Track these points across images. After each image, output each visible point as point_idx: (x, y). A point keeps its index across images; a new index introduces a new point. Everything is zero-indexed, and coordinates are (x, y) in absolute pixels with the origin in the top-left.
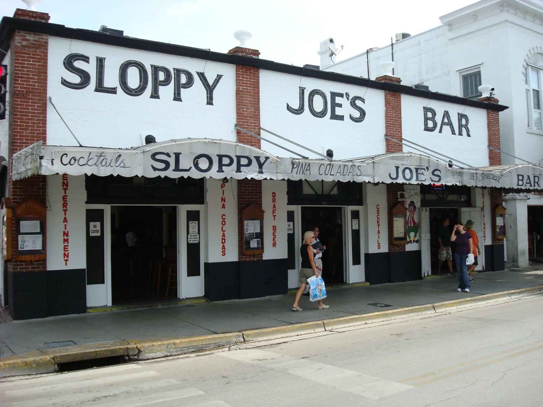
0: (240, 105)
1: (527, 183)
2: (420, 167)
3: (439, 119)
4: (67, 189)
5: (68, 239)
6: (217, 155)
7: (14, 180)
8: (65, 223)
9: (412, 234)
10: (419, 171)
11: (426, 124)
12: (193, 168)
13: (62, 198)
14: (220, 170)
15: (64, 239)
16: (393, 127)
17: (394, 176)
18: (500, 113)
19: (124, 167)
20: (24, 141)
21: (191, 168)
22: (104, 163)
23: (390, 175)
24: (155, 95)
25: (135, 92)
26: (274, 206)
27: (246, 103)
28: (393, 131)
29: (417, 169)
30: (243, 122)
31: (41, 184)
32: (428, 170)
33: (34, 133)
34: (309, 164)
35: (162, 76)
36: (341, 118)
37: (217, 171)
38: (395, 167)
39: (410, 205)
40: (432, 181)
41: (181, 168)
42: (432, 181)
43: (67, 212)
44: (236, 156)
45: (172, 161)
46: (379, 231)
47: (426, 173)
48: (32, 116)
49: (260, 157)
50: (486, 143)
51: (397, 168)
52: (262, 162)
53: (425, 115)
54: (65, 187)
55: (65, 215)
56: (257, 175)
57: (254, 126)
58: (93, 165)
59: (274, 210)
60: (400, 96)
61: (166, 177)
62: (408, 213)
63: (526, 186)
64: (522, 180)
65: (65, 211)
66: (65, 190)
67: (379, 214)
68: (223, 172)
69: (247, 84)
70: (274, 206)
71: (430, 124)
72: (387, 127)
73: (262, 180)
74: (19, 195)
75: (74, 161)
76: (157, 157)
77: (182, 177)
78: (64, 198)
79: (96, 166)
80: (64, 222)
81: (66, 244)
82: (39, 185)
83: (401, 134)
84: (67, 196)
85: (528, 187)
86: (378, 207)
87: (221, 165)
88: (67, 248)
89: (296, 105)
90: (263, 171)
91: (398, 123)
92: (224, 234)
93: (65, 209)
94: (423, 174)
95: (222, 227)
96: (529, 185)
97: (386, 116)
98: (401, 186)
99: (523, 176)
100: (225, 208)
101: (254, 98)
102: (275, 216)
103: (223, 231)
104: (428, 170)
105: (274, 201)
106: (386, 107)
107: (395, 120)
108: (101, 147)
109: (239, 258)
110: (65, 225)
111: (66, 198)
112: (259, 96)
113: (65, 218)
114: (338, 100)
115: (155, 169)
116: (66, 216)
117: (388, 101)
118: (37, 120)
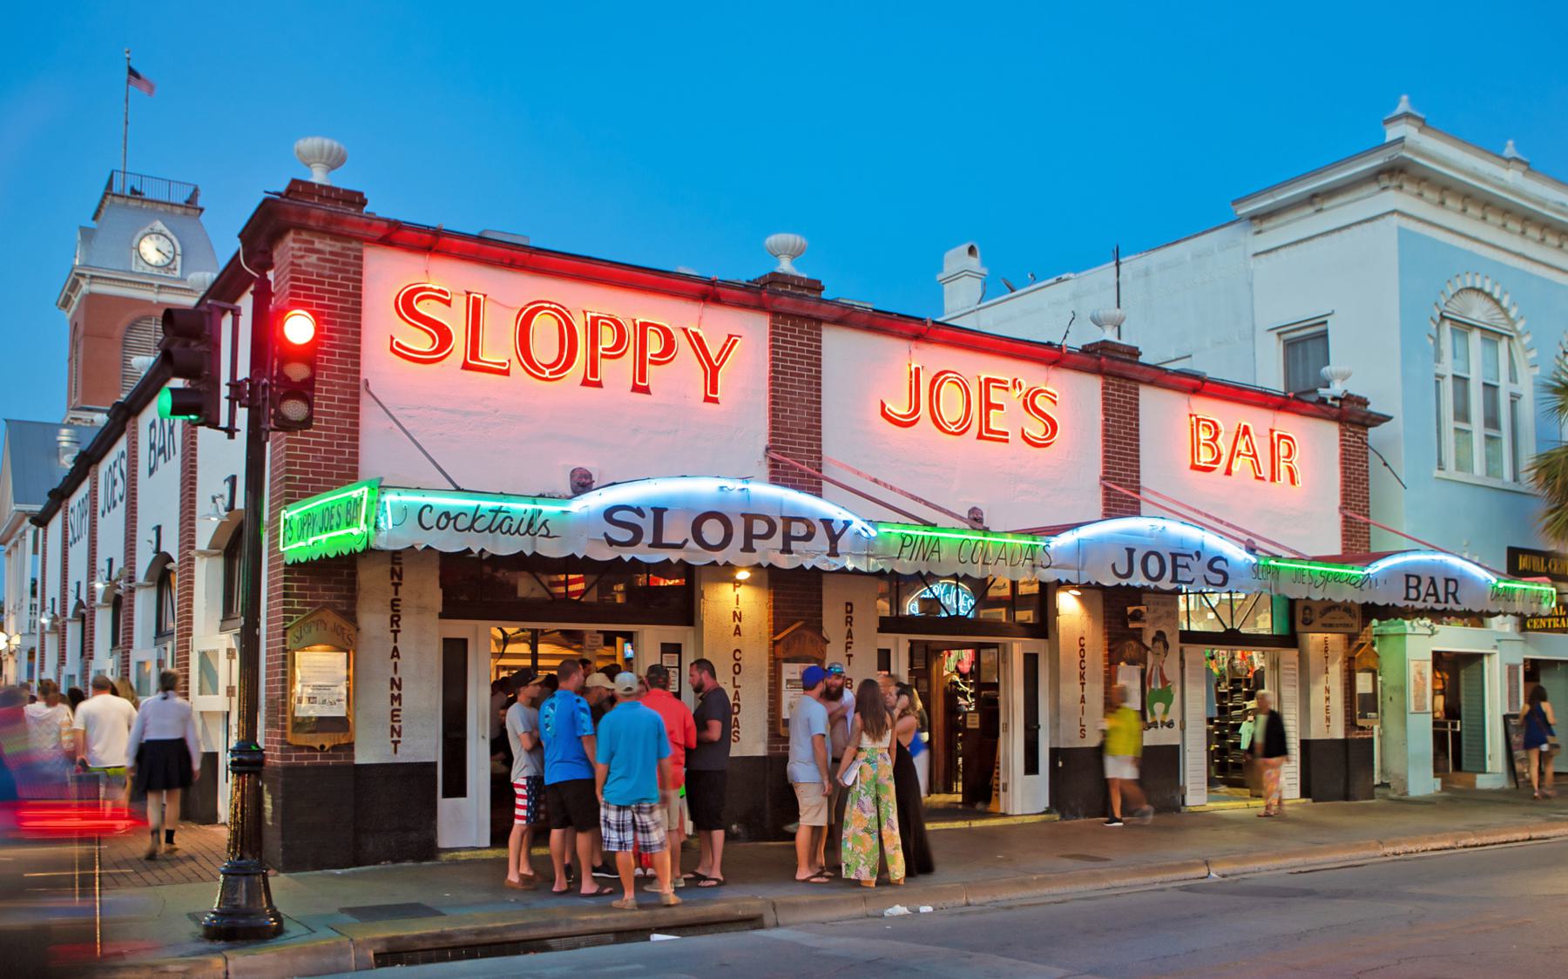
0: (777, 404)
1: (1427, 594)
2: (1181, 551)
3: (1224, 444)
4: (401, 584)
5: (400, 695)
6: (743, 515)
7: (289, 563)
8: (395, 659)
10: (1180, 561)
11: (1194, 453)
12: (692, 544)
13: (389, 603)
15: (393, 695)
16: (1119, 459)
17: (1123, 570)
18: (1371, 430)
19: (547, 536)
20: (311, 476)
21: (686, 541)
22: (505, 528)
23: (1113, 566)
24: (591, 381)
25: (551, 373)
26: (850, 635)
27: (791, 399)
28: (1120, 469)
29: (1174, 556)
30: (783, 442)
31: (345, 571)
32: (1199, 559)
33: (332, 460)
34: (938, 539)
35: (607, 338)
36: (1002, 437)
37: (742, 550)
38: (1127, 549)
39: (1154, 640)
40: (1208, 582)
41: (665, 540)
42: (1208, 582)
43: (399, 635)
44: (782, 517)
45: (647, 525)
46: (1083, 697)
47: (1193, 563)
48: (326, 421)
49: (832, 520)
50: (1337, 500)
51: (1131, 551)
52: (837, 533)
53: (1194, 432)
54: (396, 580)
55: (396, 641)
56: (826, 561)
57: (808, 451)
58: (485, 530)
59: (848, 643)
60: (1138, 389)
61: (633, 559)
62: (1150, 658)
63: (1424, 601)
64: (1417, 588)
65: (395, 632)
66: (397, 585)
67: (1085, 659)
68: (754, 551)
69: (794, 356)
70: (850, 635)
71: (1205, 457)
72: (1107, 458)
73: (825, 577)
74: (296, 596)
75: (446, 521)
76: (617, 516)
77: (668, 561)
78: (394, 604)
79: (491, 532)
80: (393, 656)
81: (396, 705)
82: (342, 575)
83: (1138, 477)
84: (399, 600)
85: (1431, 601)
86: (1082, 642)
87: (749, 536)
88: (398, 716)
89: (900, 408)
90: (839, 551)
91: (1131, 450)
92: (737, 693)
93: (395, 628)
94: (1187, 566)
95: (734, 678)
96: (1434, 598)
97: (1107, 434)
98: (1136, 594)
99: (1418, 578)
100: (740, 634)
101: (811, 389)
102: (851, 655)
103: (735, 686)
104: (1199, 559)
105: (849, 621)
106: (1105, 414)
107: (1125, 444)
108: (501, 493)
109: (770, 748)
110: (396, 664)
111: (398, 605)
112: (819, 384)
113: (395, 649)
114: (996, 396)
115: (611, 542)
116: (397, 644)
117: (1108, 399)
118: (339, 430)
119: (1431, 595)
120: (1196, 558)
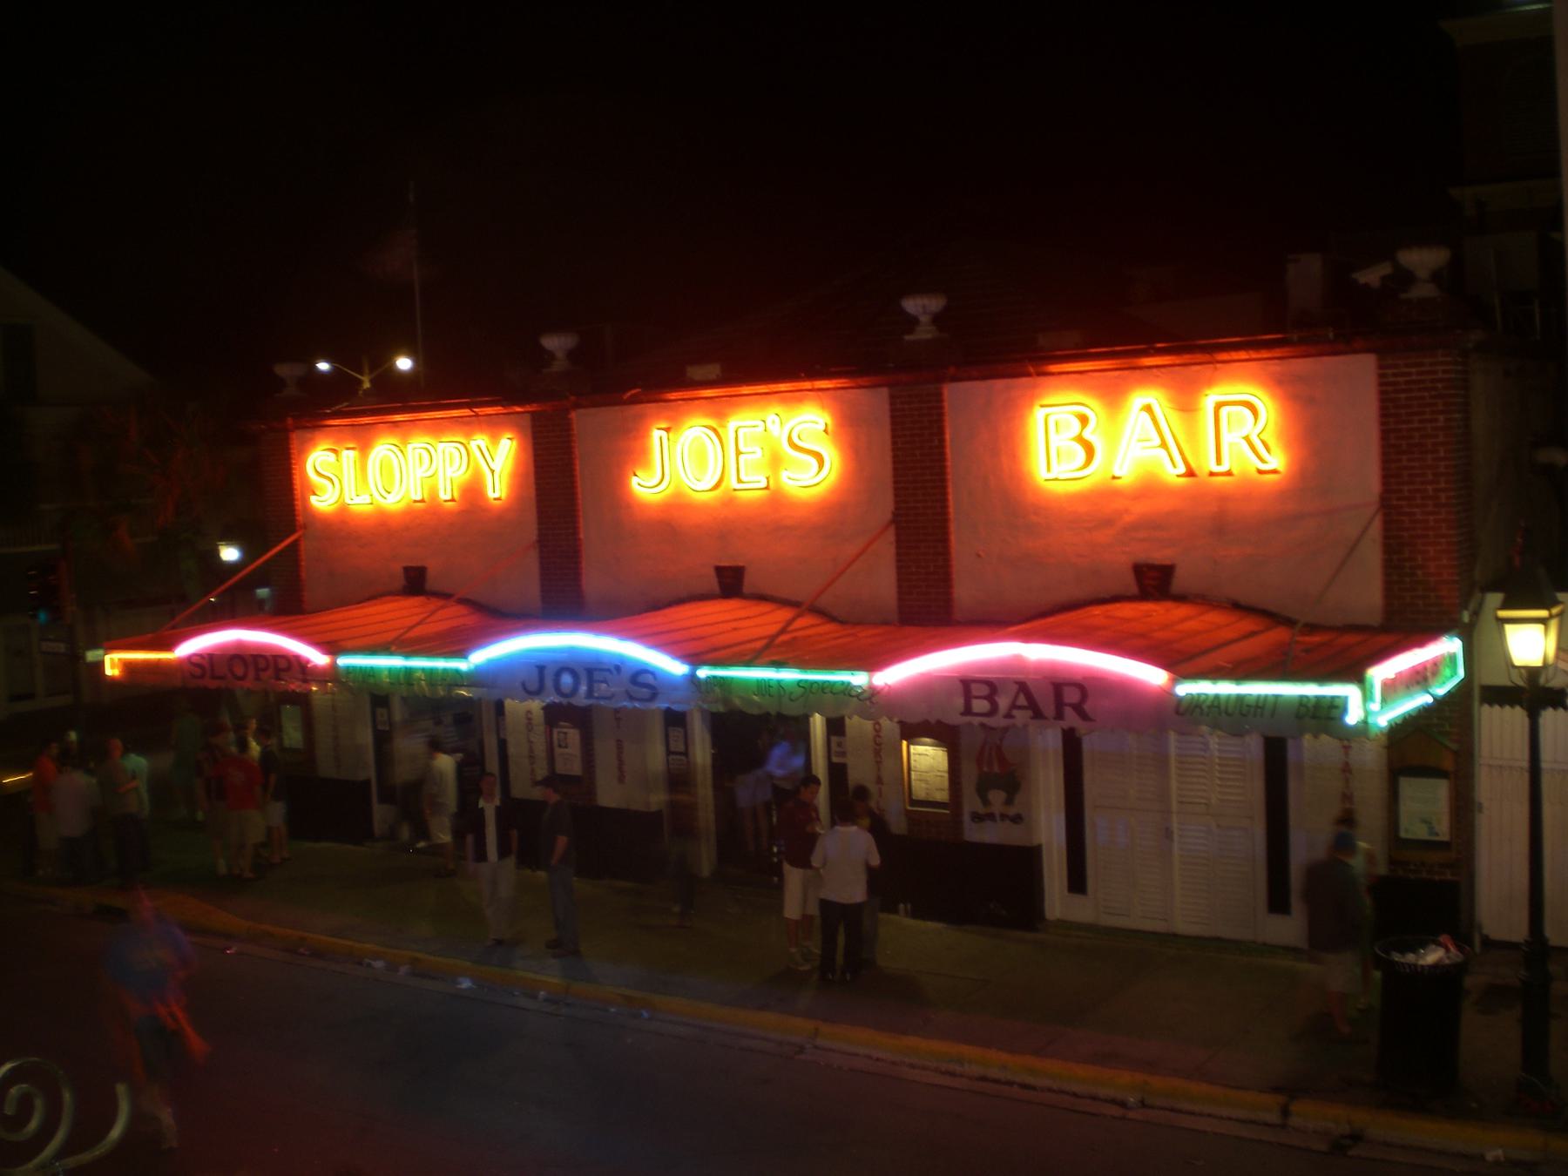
9: (997, 797)
10: (597, 676)
14: (258, 678)
64: (991, 698)
94: (605, 681)
119: (1020, 708)
120: (615, 672)
